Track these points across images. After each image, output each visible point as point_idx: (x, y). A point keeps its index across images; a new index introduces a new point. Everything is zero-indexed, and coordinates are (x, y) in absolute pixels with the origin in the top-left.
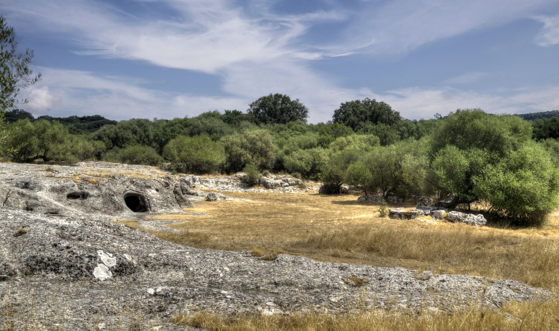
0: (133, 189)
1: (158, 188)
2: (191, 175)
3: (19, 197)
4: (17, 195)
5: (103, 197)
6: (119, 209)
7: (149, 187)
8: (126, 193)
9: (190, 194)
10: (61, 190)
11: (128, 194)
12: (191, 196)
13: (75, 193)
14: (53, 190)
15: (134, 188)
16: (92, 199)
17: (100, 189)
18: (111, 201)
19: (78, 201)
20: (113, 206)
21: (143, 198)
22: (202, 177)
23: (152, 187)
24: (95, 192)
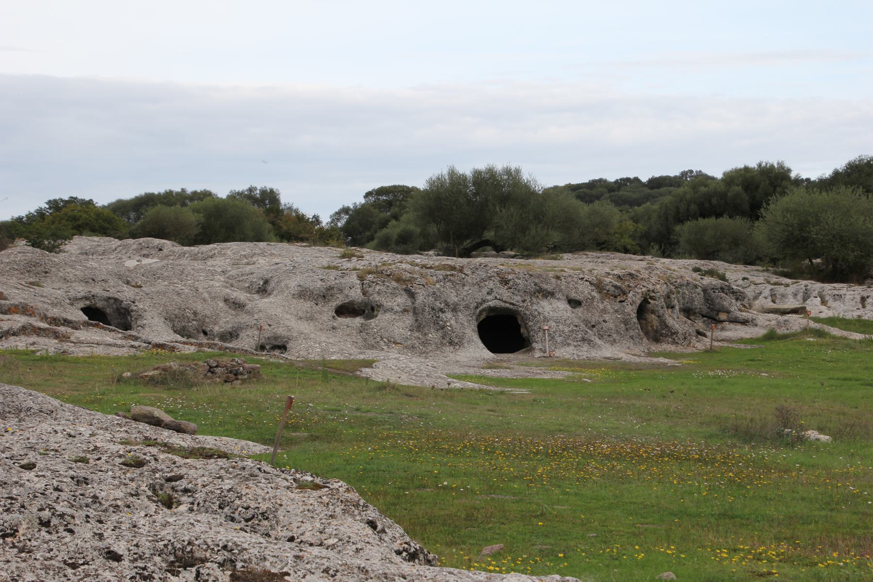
0: (502, 297)
1: (579, 297)
3: (226, 308)
4: (221, 304)
5: (415, 313)
6: (451, 343)
7: (548, 294)
8: (485, 306)
9: (735, 321)
10: (325, 296)
11: (491, 309)
12: (739, 327)
13: (351, 303)
14: (303, 294)
15: (504, 293)
16: (388, 316)
17: (412, 295)
18: (436, 323)
19: (358, 321)
20: (440, 333)
21: (525, 319)
22: (827, 286)
23: (559, 295)
24: (402, 300)
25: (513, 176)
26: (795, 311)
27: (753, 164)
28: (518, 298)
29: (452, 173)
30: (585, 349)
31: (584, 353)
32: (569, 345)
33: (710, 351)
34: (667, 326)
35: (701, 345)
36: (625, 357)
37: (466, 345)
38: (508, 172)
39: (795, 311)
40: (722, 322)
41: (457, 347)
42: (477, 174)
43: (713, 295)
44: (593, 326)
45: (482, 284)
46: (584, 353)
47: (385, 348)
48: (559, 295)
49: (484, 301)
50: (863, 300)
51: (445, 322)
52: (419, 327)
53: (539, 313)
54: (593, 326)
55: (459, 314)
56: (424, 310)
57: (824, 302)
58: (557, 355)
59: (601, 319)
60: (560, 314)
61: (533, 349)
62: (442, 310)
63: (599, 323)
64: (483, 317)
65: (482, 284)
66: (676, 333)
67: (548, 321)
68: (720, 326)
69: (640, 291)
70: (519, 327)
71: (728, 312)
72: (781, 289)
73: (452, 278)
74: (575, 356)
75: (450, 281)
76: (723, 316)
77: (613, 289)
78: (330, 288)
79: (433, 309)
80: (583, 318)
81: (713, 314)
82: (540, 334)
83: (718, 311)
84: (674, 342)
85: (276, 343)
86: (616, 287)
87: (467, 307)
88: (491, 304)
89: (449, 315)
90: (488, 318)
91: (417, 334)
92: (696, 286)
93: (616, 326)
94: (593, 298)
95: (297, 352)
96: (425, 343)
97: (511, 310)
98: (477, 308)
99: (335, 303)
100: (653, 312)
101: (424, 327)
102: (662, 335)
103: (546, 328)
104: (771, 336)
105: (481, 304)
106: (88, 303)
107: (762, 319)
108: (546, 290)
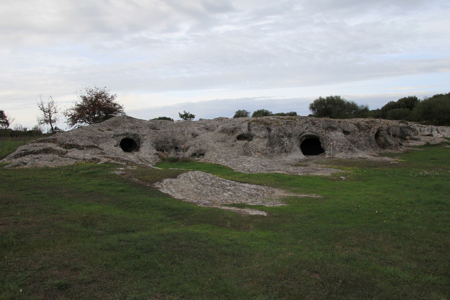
2: (431, 126)
5: (269, 138)
6: (286, 152)
10: (233, 132)
11: (307, 136)
12: (414, 141)
15: (314, 129)
16: (257, 140)
17: (269, 130)
18: (279, 142)
19: (246, 141)
20: (281, 147)
22: (439, 128)
24: (264, 132)
25: (338, 98)
26: (429, 135)
27: (407, 97)
28: (320, 131)
29: (320, 98)
30: (350, 153)
31: (349, 155)
32: (342, 152)
33: (407, 152)
34: (388, 142)
35: (402, 150)
36: (369, 157)
38: (337, 97)
39: (429, 135)
40: (407, 139)
42: (328, 98)
43: (404, 130)
44: (355, 143)
46: (349, 155)
47: (253, 154)
49: (304, 132)
52: (270, 144)
53: (329, 137)
54: (355, 143)
55: (292, 138)
56: (274, 137)
57: (438, 132)
58: (336, 156)
62: (282, 137)
64: (304, 139)
66: (392, 145)
68: (406, 141)
70: (320, 143)
71: (410, 136)
72: (423, 129)
74: (345, 157)
75: (290, 124)
76: (408, 137)
78: (236, 128)
79: (278, 136)
81: (404, 137)
82: (329, 147)
83: (406, 136)
84: (391, 149)
85: (201, 153)
86: (366, 126)
87: (296, 135)
89: (286, 139)
90: (306, 140)
91: (269, 148)
92: (398, 127)
94: (355, 130)
95: (210, 157)
96: (272, 152)
98: (300, 135)
99: (237, 134)
100: (382, 136)
101: (273, 144)
102: (386, 145)
104: (427, 145)
105: (303, 134)
106: (125, 136)
107: (423, 138)
108: (333, 127)
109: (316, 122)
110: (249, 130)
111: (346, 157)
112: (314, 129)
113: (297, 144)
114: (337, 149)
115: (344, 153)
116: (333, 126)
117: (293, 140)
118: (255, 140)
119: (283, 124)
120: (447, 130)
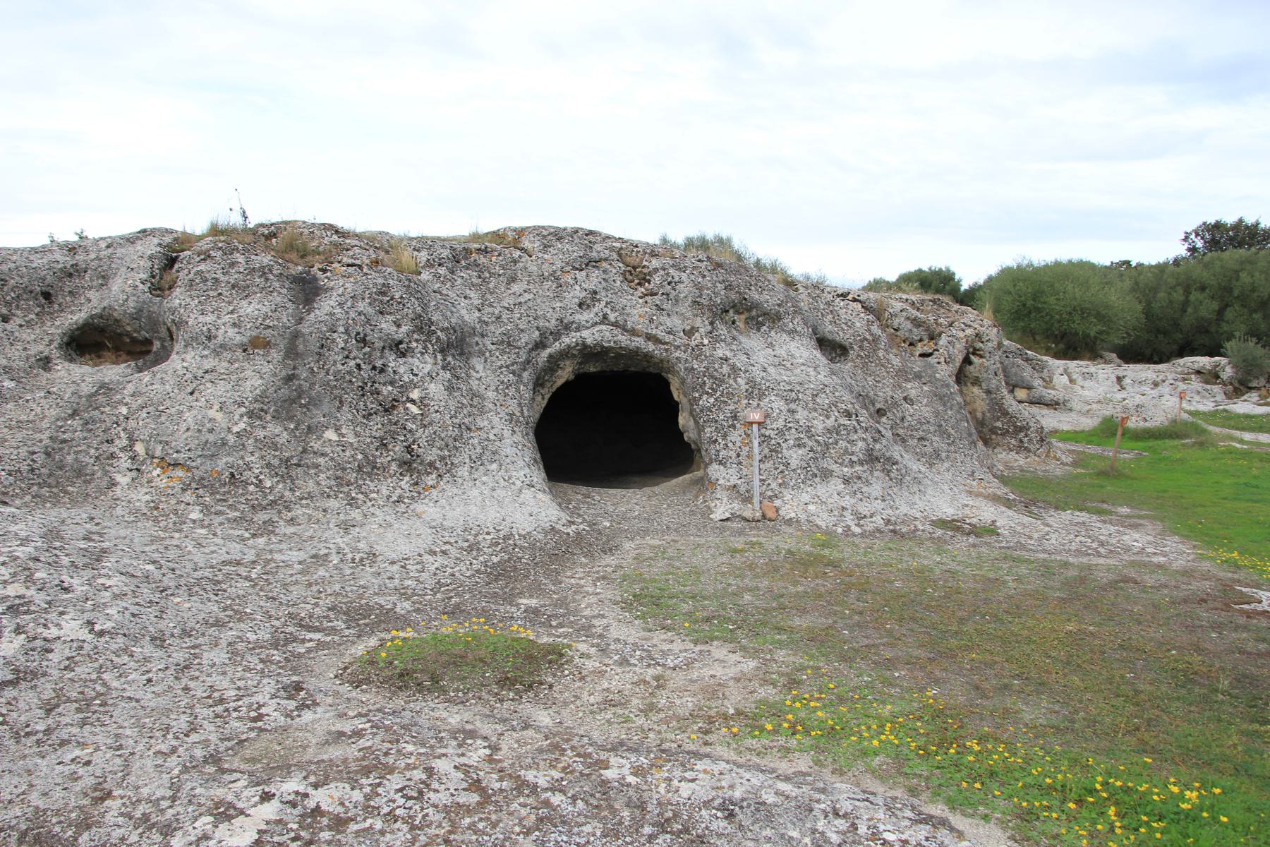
1: (842, 336)
5: (292, 352)
6: (410, 464)
8: (569, 340)
11: (588, 353)
15: (637, 310)
22: (1072, 365)
30: (876, 489)
32: (826, 475)
34: (1006, 413)
37: (463, 472)
41: (431, 480)
44: (880, 413)
45: (568, 278)
47: (123, 480)
48: (797, 323)
49: (567, 326)
50: (1119, 379)
51: (405, 388)
52: (291, 402)
53: (734, 369)
54: (880, 413)
55: (477, 363)
58: (788, 511)
59: (899, 395)
60: (797, 375)
61: (704, 484)
62: (398, 348)
63: (896, 404)
64: (565, 374)
65: (568, 278)
66: (1025, 428)
67: (761, 396)
69: (961, 334)
70: (674, 408)
71: (1029, 388)
73: (482, 259)
74: (849, 520)
77: (909, 325)
79: (363, 341)
80: (856, 389)
82: (735, 437)
84: (1021, 448)
86: (916, 322)
87: (507, 343)
88: (590, 336)
89: (423, 364)
90: (580, 382)
91: (274, 428)
93: (937, 414)
94: (876, 340)
96: (287, 469)
97: (648, 357)
98: (540, 345)
99: (76, 317)
100: (976, 382)
101: (314, 402)
102: (993, 430)
103: (756, 416)
105: (557, 335)
108: (755, 306)
109: (655, 263)
110: (159, 287)
111: (860, 517)
112: (637, 310)
113: (513, 406)
114: (795, 457)
115: (836, 485)
116: (755, 295)
117: (484, 374)
118: (183, 361)
119: (429, 264)
120: (1101, 376)
